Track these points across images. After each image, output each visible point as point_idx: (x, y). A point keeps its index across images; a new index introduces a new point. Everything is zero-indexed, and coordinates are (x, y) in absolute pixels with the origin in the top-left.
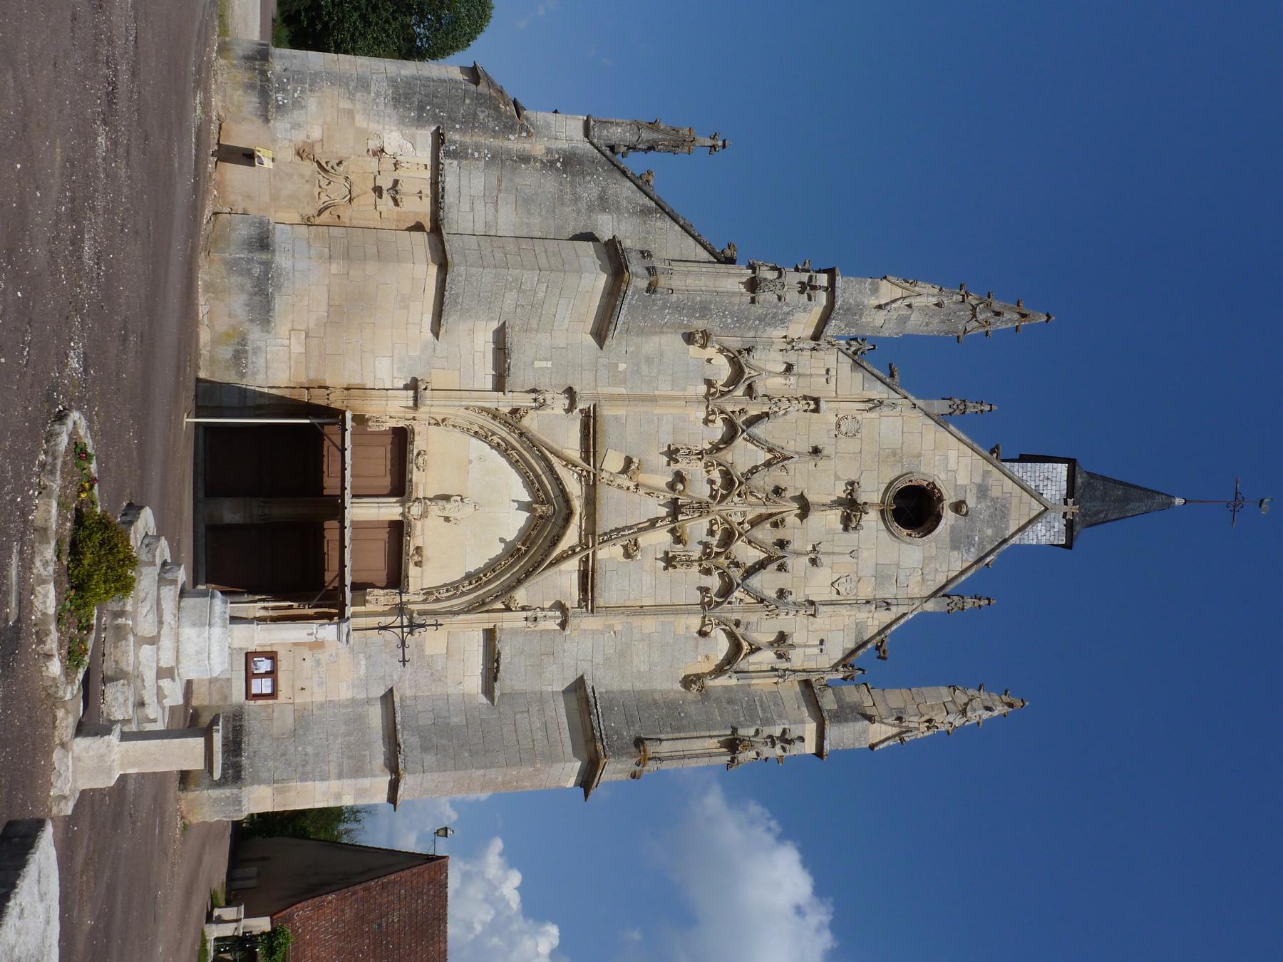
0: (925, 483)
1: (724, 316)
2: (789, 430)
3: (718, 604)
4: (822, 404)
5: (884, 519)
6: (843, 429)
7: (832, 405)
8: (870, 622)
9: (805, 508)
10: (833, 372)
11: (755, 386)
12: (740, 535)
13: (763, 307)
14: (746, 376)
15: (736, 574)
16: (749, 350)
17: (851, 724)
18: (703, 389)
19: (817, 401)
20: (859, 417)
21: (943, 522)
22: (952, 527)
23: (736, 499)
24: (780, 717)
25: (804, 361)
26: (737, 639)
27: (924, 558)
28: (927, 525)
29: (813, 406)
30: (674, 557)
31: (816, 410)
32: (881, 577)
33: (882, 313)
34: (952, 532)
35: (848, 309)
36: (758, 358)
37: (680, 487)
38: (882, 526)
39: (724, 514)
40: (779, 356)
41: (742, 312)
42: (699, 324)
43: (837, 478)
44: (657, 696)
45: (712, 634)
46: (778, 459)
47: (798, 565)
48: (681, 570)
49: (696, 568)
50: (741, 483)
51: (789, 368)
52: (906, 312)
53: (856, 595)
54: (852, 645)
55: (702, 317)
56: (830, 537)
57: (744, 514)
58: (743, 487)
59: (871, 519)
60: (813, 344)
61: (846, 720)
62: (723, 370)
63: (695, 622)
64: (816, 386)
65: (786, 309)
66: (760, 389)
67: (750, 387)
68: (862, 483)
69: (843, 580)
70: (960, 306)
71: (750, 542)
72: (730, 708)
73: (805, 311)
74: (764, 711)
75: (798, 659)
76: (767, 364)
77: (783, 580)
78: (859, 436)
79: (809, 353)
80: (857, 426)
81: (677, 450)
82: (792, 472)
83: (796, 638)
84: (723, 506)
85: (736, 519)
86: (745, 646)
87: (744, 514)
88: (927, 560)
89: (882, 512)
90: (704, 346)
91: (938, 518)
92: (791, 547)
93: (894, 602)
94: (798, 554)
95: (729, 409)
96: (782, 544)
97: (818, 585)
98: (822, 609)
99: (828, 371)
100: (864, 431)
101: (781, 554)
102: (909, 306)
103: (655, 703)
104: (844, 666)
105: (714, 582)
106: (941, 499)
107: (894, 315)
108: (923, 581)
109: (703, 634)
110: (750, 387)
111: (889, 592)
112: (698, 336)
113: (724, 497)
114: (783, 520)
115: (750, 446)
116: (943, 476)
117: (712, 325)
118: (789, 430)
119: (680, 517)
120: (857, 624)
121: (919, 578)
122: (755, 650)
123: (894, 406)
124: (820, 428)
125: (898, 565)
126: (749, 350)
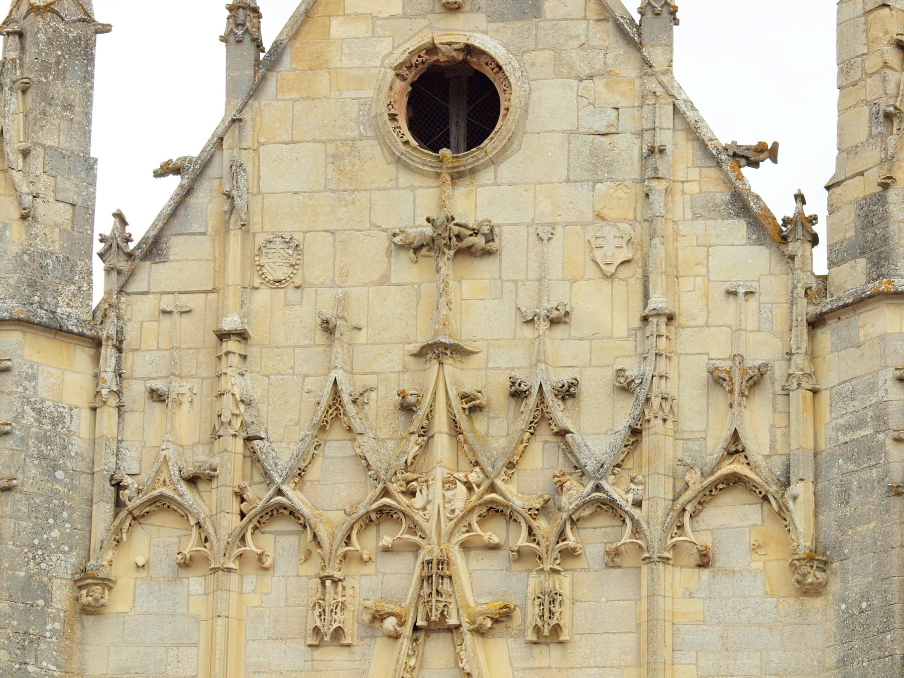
0: (399, 84)
1: (44, 546)
2: (282, 394)
3: (637, 530)
4: (231, 323)
5: (473, 171)
6: (281, 273)
7: (232, 301)
8: (692, 188)
9: (436, 351)
10: (167, 303)
11: (190, 470)
12: (492, 488)
13: (23, 468)
14: (167, 491)
15: (576, 492)
16: (118, 486)
17: (893, 228)
18: (195, 583)
19: (223, 336)
20: (260, 239)
21: (479, 41)
22: (491, 18)
23: (418, 501)
24: (872, 388)
25: (145, 366)
26: (715, 484)
27: (558, 76)
28: (488, 71)
29: (232, 345)
30: (537, 630)
31: (242, 336)
32: (598, 169)
33: (41, 208)
34: (503, 18)
35: (32, 284)
36: (137, 467)
37: (390, 623)
38: (487, 176)
39: (446, 526)
40: (132, 420)
41: (35, 509)
42: (61, 595)
43: (385, 280)
44: (832, 659)
45: (705, 540)
46: (335, 411)
47: (563, 357)
48: (565, 615)
49: (564, 584)
50: (386, 493)
51: (157, 396)
52: (37, 162)
53: (633, 222)
54: (740, 226)
55: (46, 592)
56: (508, 286)
57: (449, 483)
58: (394, 488)
59: (472, 204)
60: (108, 353)
61: (885, 240)
62: (154, 542)
63: (679, 579)
64: (194, 332)
65: (30, 417)
66: (197, 458)
67: (193, 480)
68: (394, 225)
69: (599, 255)
70: (29, 38)
71: (511, 465)
72: (856, 499)
73: (33, 378)
74: (862, 424)
75: (762, 349)
76: (155, 445)
77: (595, 387)
78: (298, 237)
79: (129, 358)
80: (278, 244)
81: (316, 630)
82: (370, 380)
83: (719, 352)
84: (430, 527)
85: (460, 498)
86: (728, 468)
87: (449, 483)
88: (563, 69)
89: (457, 176)
90: (107, 583)
91: (469, 49)
92: (520, 375)
93: (647, 136)
94: (539, 360)
95: (236, 522)
96: (518, 394)
97: (605, 313)
98: (657, 301)
99: (165, 312)
100: (288, 227)
101: (533, 399)
102: (25, 153)
103: (843, 662)
104: (784, 239)
105: (593, 539)
106: (432, 49)
107: (44, 184)
108: (607, 73)
109: (704, 561)
110: (193, 480)
111: (627, 149)
112: (86, 599)
113: (414, 528)
114: (465, 397)
115: (313, 474)
116: (385, 46)
117: (64, 565)
118: (282, 394)
119: (452, 621)
120: (696, 216)
121: (599, 85)
122: (735, 447)
123: (236, 168)
124: (282, 322)
125: (572, 133)
126: (118, 486)
